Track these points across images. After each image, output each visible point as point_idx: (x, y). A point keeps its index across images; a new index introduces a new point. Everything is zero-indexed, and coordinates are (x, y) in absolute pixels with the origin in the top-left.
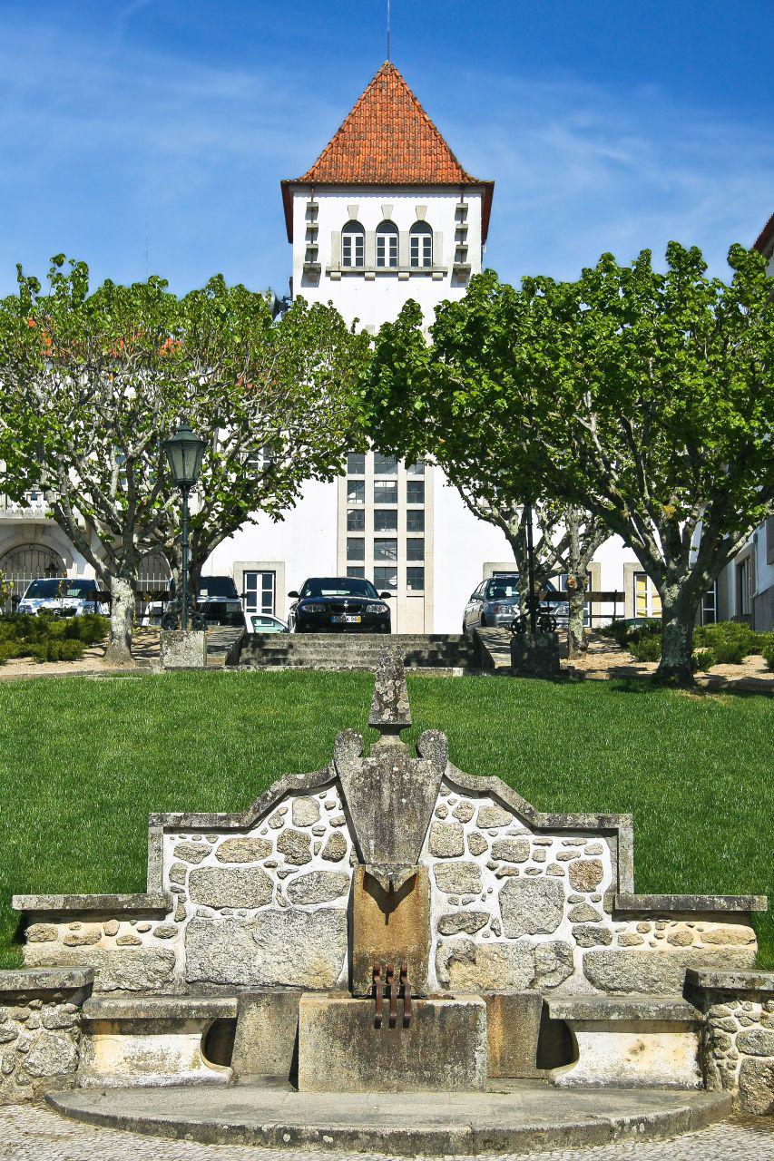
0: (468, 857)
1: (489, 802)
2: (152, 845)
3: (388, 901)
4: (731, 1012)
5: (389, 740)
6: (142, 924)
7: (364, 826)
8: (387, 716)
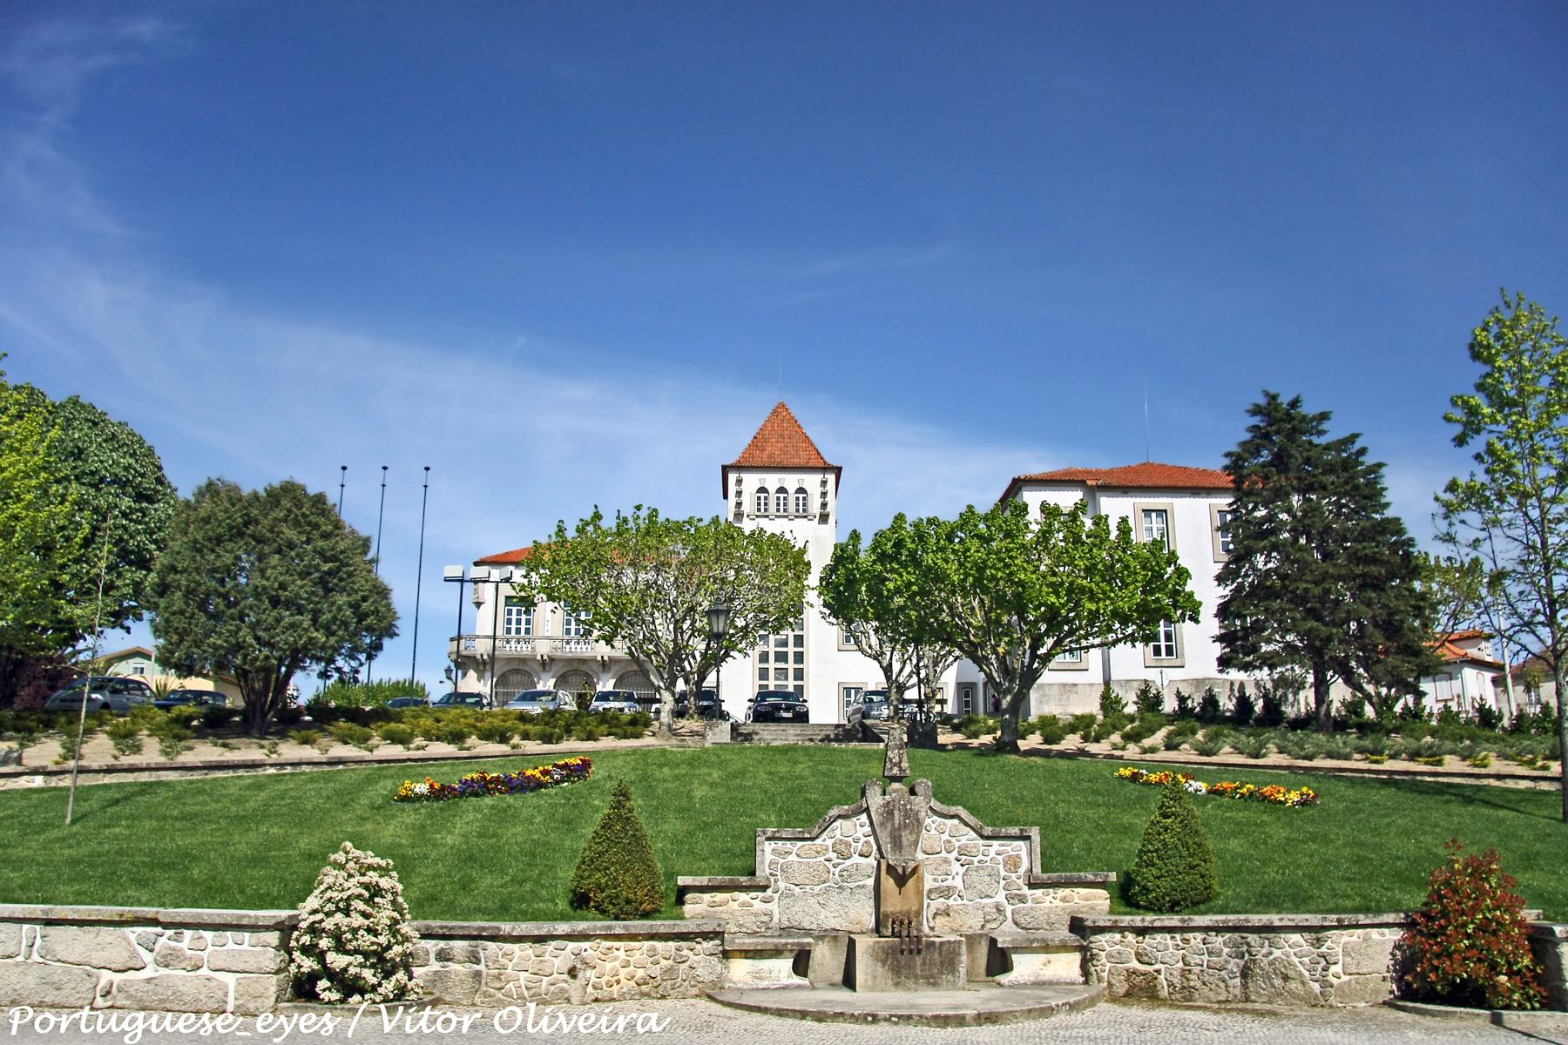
0: (944, 854)
1: (956, 821)
2: (758, 848)
3: (901, 880)
4: (1102, 940)
5: (896, 785)
6: (753, 894)
7: (884, 837)
8: (895, 771)
